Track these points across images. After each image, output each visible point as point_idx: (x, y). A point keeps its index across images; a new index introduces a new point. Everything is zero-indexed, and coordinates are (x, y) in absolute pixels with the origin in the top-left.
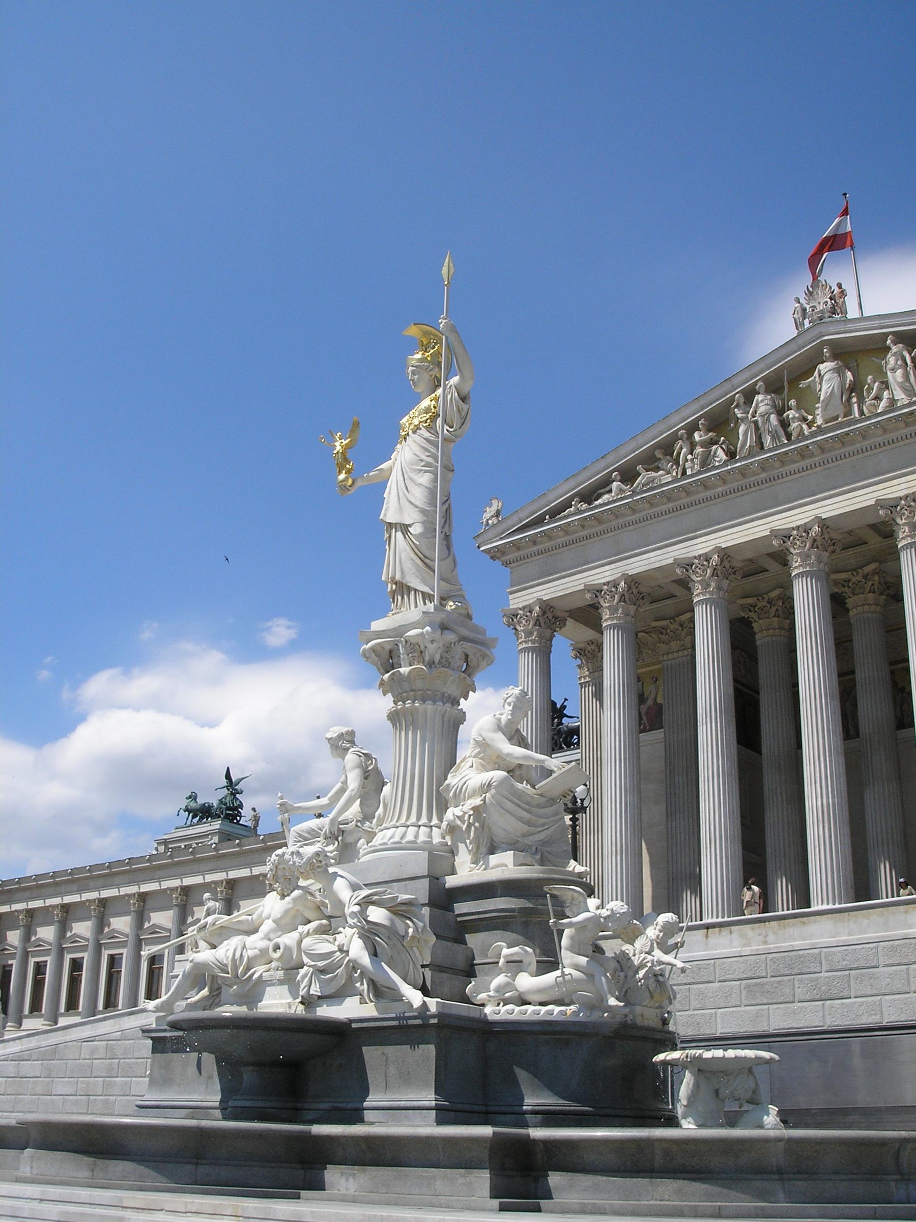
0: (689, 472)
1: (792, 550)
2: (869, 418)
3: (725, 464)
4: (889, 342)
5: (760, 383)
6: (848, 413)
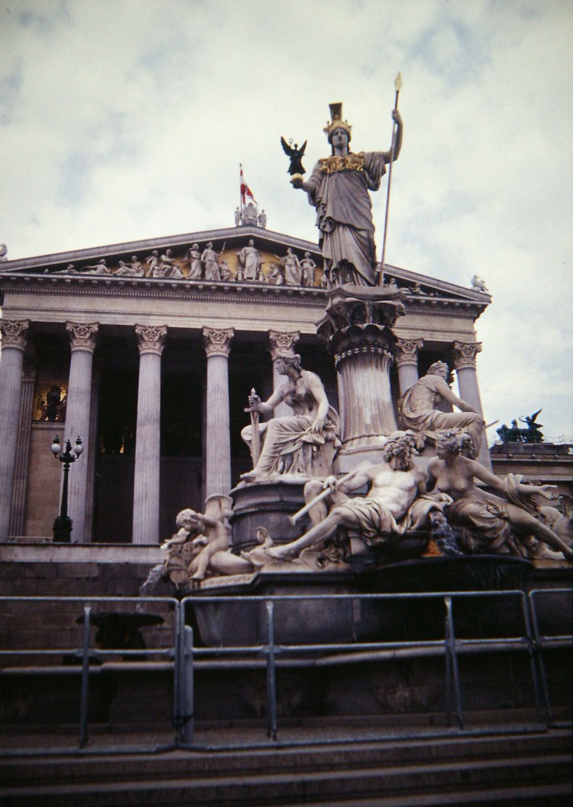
0: (154, 276)
2: (274, 285)
4: (289, 251)
5: (210, 243)
6: (257, 278)
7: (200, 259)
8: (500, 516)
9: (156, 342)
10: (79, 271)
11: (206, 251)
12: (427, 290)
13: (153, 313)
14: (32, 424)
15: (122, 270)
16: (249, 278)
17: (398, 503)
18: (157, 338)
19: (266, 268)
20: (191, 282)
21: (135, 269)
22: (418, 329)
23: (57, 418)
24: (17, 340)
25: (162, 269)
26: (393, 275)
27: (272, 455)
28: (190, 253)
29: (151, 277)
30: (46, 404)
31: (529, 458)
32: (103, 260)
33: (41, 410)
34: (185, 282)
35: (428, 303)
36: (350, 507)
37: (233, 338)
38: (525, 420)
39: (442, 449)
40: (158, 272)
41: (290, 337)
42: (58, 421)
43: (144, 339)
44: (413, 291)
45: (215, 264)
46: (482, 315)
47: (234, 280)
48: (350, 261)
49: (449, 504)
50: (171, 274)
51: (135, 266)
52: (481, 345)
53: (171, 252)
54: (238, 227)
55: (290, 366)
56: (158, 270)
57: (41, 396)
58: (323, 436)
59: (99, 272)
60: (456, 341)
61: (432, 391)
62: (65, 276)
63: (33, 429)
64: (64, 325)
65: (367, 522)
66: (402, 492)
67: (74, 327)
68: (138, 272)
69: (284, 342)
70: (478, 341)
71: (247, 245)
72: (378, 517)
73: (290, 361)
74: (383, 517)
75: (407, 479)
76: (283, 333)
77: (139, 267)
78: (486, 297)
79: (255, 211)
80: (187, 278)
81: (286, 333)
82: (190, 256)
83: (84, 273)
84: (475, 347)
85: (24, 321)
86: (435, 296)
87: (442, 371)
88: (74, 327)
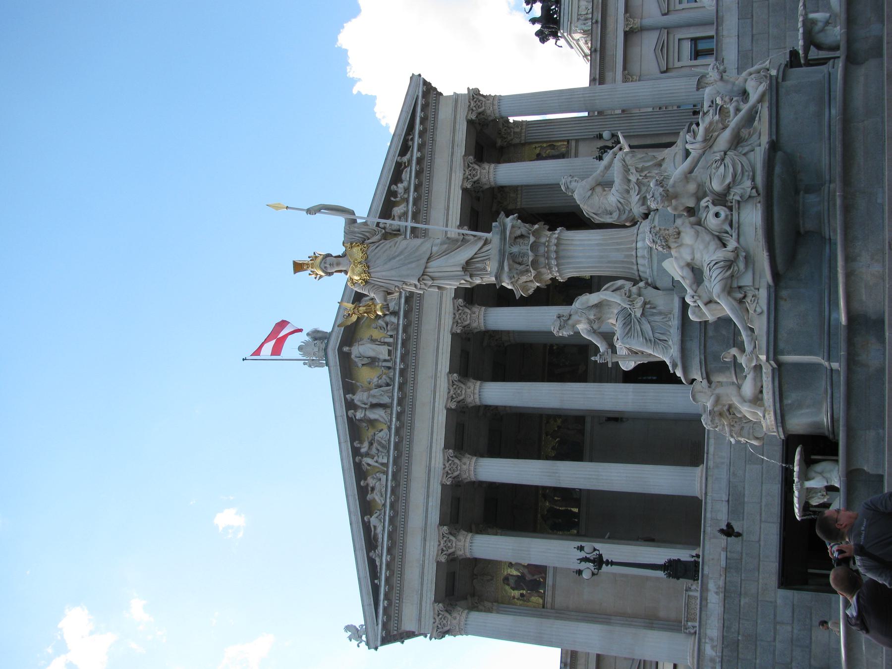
0: (385, 461)
1: (461, 398)
2: (398, 324)
3: (389, 428)
5: (347, 396)
6: (388, 344)
7: (366, 409)
8: (723, 160)
9: (461, 462)
10: (375, 547)
11: (356, 401)
12: (405, 149)
13: (428, 465)
14: (547, 608)
15: (376, 497)
16: (390, 352)
17: (709, 244)
18: (457, 461)
19: (376, 334)
20: (394, 420)
21: (376, 483)
22: (452, 161)
23: (542, 580)
24: (456, 617)
25: (377, 452)
26: (387, 188)
27: (653, 344)
28: (358, 420)
29: (386, 465)
30: (524, 592)
31: (597, 27)
32: (366, 519)
33: (531, 597)
34: (393, 427)
35: (421, 148)
36: (714, 284)
37: (460, 374)
38: (529, 6)
39: (664, 204)
40: (381, 457)
41: (459, 310)
42: (545, 579)
43: (458, 475)
44: (406, 164)
45: (372, 392)
46: (433, 85)
47: (392, 370)
48: (463, 262)
49: (711, 201)
50: (383, 442)
51: (372, 482)
52: (471, 88)
53: (357, 442)
54: (327, 364)
55: (567, 324)
56: (378, 456)
57: (514, 598)
58: (637, 298)
59: (381, 526)
60: (467, 116)
61: (592, 194)
62: (384, 561)
63: (553, 608)
64: (438, 563)
65: (727, 271)
66: (699, 238)
67: (442, 553)
68: (380, 479)
69: (464, 316)
70: (466, 92)
71: (349, 354)
72: (723, 263)
73: (562, 323)
74: (722, 259)
75: (688, 237)
76: (454, 318)
77: (374, 478)
78: (414, 79)
79: (307, 344)
80: (389, 424)
81: (454, 314)
82: (361, 420)
83: (380, 540)
84: (473, 96)
85: (434, 609)
86: (412, 139)
87: (571, 182)
88: (442, 553)
